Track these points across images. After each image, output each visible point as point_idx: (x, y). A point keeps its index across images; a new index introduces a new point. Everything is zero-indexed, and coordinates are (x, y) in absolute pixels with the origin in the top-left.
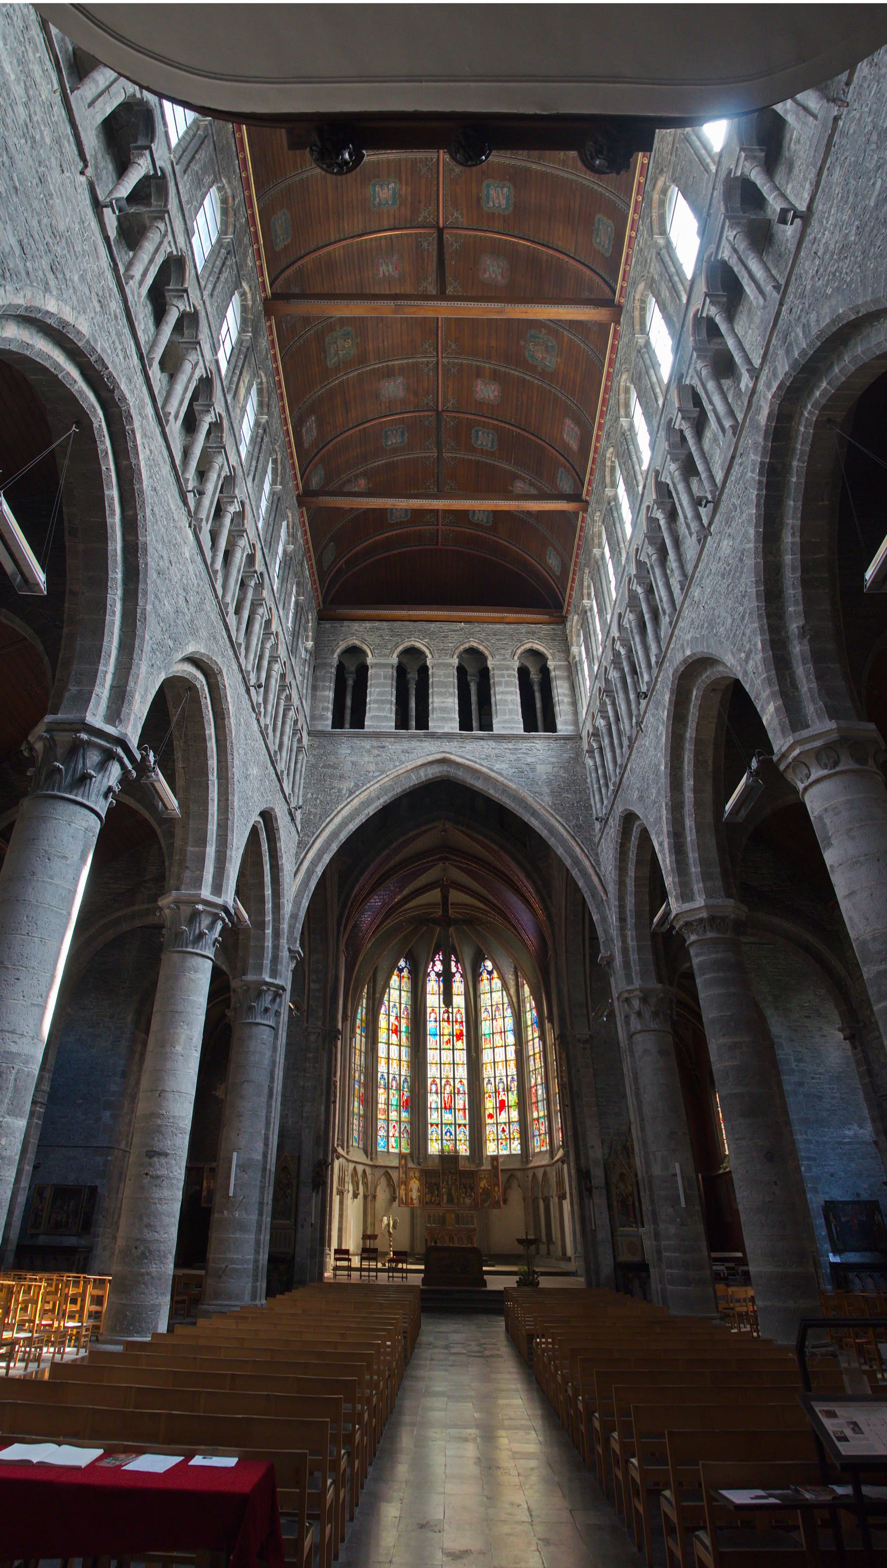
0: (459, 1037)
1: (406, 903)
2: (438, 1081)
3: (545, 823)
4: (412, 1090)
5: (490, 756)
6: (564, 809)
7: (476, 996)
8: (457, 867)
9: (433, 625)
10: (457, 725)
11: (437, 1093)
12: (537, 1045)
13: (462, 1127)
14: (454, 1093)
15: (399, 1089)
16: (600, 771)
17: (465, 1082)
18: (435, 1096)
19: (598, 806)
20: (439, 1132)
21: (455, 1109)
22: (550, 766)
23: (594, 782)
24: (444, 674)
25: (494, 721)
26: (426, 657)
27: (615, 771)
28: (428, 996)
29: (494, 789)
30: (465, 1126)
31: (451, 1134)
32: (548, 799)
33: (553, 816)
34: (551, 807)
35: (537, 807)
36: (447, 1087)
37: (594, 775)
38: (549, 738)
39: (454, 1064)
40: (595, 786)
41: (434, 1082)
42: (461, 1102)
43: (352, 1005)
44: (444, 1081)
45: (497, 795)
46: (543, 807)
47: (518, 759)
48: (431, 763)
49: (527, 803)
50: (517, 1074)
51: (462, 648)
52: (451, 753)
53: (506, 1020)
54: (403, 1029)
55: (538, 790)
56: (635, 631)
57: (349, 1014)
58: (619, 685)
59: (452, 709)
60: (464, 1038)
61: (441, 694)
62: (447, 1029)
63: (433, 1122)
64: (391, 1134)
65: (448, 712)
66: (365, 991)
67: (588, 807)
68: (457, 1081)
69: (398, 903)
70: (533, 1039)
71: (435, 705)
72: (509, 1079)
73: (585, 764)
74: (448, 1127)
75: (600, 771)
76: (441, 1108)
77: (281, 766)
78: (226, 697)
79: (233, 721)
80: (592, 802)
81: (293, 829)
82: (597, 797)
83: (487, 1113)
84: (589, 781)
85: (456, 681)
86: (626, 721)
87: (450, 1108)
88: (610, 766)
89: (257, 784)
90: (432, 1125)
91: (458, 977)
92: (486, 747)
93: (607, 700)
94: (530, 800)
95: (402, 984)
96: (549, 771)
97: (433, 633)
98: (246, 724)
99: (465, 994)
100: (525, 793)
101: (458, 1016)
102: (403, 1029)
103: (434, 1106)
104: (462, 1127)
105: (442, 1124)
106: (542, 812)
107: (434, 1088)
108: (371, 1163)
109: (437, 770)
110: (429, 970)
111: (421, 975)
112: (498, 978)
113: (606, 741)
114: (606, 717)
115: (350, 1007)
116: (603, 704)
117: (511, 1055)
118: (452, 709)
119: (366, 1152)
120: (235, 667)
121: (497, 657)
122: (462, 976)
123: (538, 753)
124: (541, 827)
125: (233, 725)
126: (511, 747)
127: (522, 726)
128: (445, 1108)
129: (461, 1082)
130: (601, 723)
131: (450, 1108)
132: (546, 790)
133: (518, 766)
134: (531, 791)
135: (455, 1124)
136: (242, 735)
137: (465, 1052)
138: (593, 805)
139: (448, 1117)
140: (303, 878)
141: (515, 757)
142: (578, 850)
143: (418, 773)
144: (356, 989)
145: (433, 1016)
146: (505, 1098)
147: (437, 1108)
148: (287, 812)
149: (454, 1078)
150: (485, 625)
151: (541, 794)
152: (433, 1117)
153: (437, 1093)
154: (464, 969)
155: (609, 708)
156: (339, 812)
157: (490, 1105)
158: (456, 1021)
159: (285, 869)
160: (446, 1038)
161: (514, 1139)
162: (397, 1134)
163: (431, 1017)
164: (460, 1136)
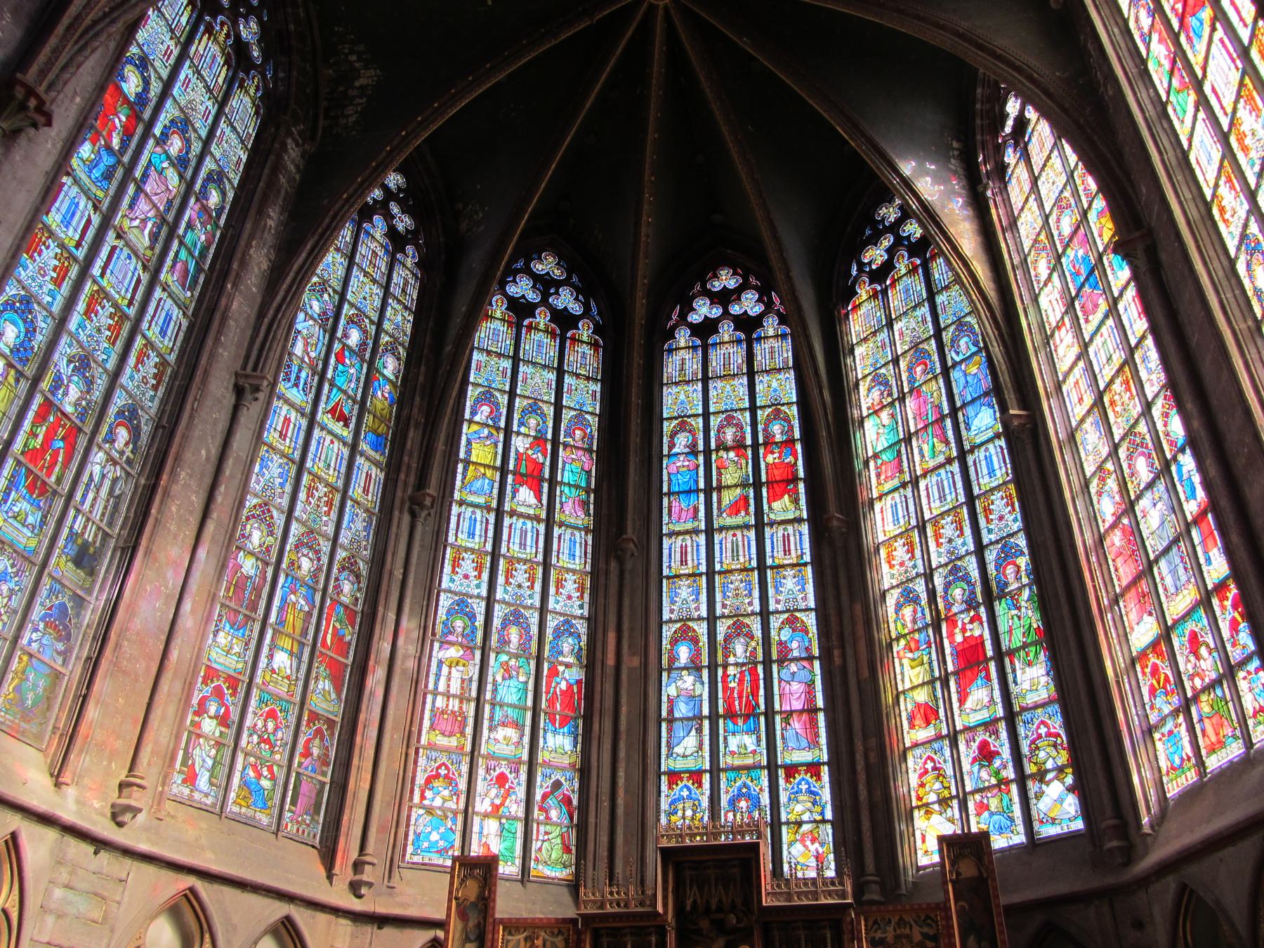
0: (782, 484)
2: (701, 629)
4: (591, 660)
7: (837, 350)
11: (695, 667)
13: (803, 778)
14: (767, 662)
17: (810, 620)
18: (688, 680)
21: (770, 714)
31: (757, 804)
36: (739, 648)
39: (762, 567)
41: (685, 634)
44: (722, 628)
50: (1028, 529)
53: (955, 375)
60: (801, 486)
62: (733, 471)
63: (679, 765)
64: (482, 805)
68: (775, 622)
74: (744, 778)
76: (714, 717)
87: (751, 713)
90: (674, 776)
101: (776, 429)
104: (803, 778)
105: (715, 771)
107: (684, 653)
108: (339, 895)
119: (328, 854)
128: (731, 715)
129: (792, 622)
135: (772, 767)
137: (805, 528)
149: (765, 614)
153: (695, 667)
154: (792, 299)
158: (769, 443)
160: (729, 497)
161: (1041, 776)
162: (517, 809)
164: (795, 808)
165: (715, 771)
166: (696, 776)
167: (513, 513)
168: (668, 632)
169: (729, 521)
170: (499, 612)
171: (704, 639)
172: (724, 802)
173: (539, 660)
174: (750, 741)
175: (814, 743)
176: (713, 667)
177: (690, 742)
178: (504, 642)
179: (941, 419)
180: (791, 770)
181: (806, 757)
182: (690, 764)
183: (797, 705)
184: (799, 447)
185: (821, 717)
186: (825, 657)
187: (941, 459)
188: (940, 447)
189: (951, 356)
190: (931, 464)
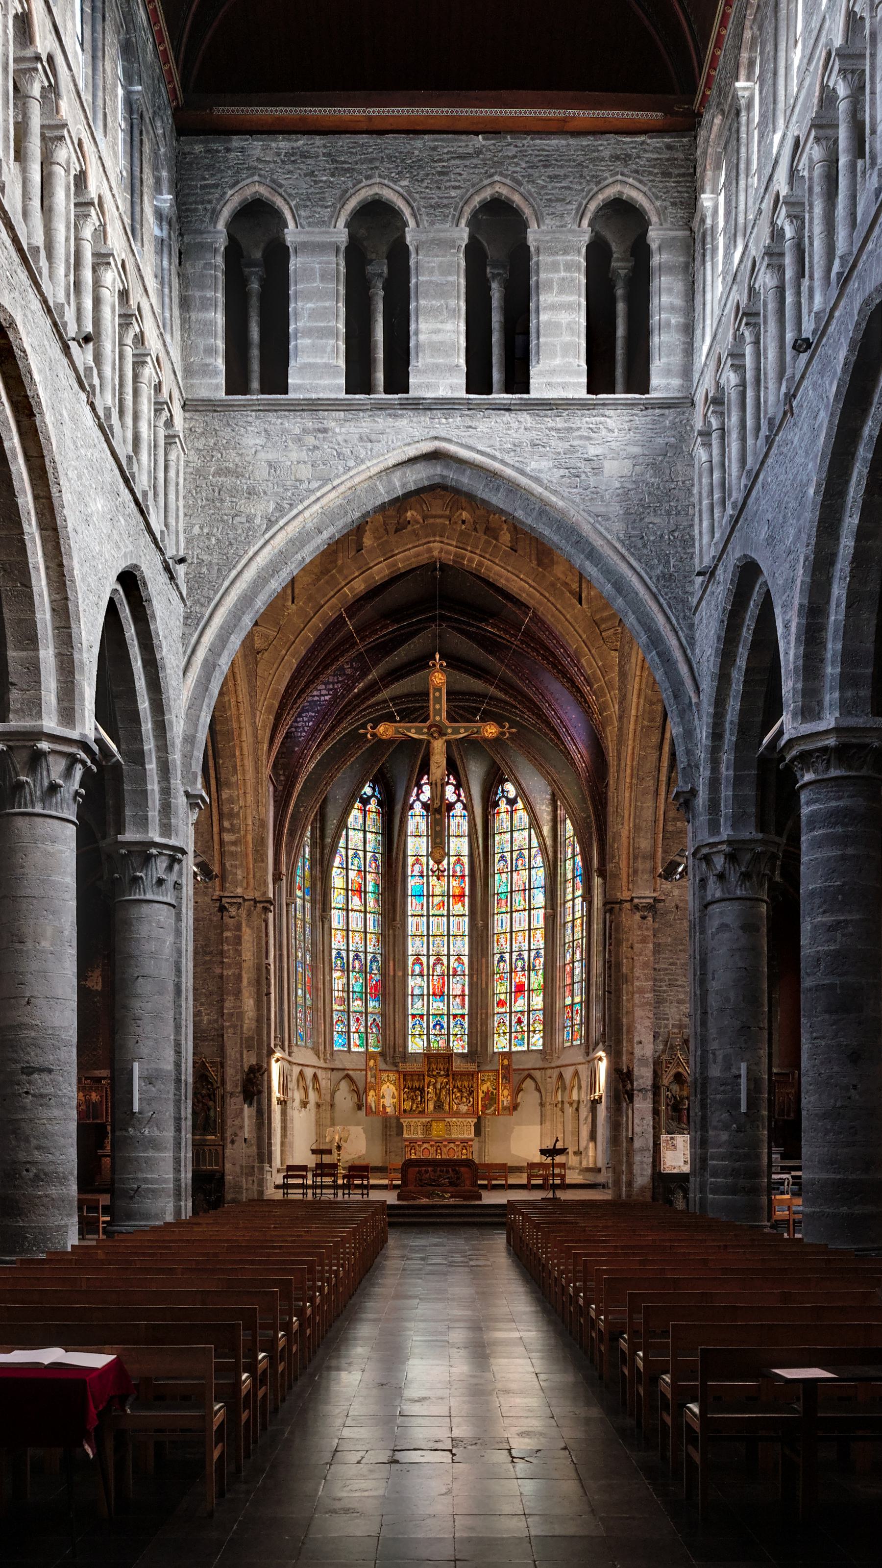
1: (373, 695)
3: (608, 572)
5: (519, 445)
6: (645, 546)
8: (462, 632)
9: (419, 143)
10: (461, 380)
12: (578, 907)
15: (364, 971)
16: (716, 475)
18: (419, 980)
19: (706, 539)
20: (425, 1025)
21: (448, 995)
22: (628, 463)
23: (705, 494)
24: (440, 266)
25: (533, 371)
26: (405, 224)
27: (740, 478)
28: (410, 840)
29: (524, 509)
30: (463, 1016)
32: (618, 527)
33: (623, 557)
34: (624, 545)
35: (598, 542)
37: (705, 481)
38: (632, 405)
40: (705, 502)
42: (459, 986)
43: (288, 854)
45: (529, 521)
46: (609, 542)
47: (573, 450)
48: (413, 461)
49: (580, 535)
51: (476, 201)
52: (449, 441)
54: (370, 888)
55: (602, 510)
56: (817, 189)
57: (284, 870)
58: (771, 306)
59: (454, 346)
61: (434, 312)
63: (415, 1012)
65: (447, 355)
66: (308, 834)
67: (688, 542)
69: (357, 696)
70: (573, 899)
71: (422, 337)
72: (533, 954)
73: (692, 458)
75: (716, 475)
76: (428, 995)
77: (142, 482)
78: (30, 372)
79: (49, 418)
80: (697, 532)
81: (174, 595)
82: (706, 524)
83: (496, 999)
84: (695, 491)
85: (463, 282)
86: (772, 385)
88: (734, 468)
89: (105, 527)
90: (414, 1016)
91: (459, 806)
92: (515, 425)
93: (747, 334)
94: (586, 529)
95: (368, 823)
96: (626, 472)
97: (419, 164)
98: (72, 419)
99: (469, 836)
100: (579, 517)
102: (370, 888)
103: (417, 991)
105: (428, 1015)
106: (607, 551)
109: (423, 475)
110: (412, 800)
111: (398, 808)
112: (525, 808)
113: (734, 420)
114: (739, 368)
115: (284, 859)
116: (739, 339)
117: (538, 920)
118: (454, 346)
120: (36, 304)
121: (548, 221)
122: (465, 808)
123: (610, 437)
124: (602, 579)
125: (50, 427)
126: (559, 426)
127: (584, 380)
128: (434, 995)
130: (731, 378)
131: (442, 995)
132: (616, 509)
133: (573, 462)
134: (589, 513)
135: (448, 1015)
136: (69, 443)
138: (697, 537)
139: (438, 1006)
140: (199, 677)
141: (567, 445)
142: (660, 619)
143: (390, 482)
144: (292, 834)
145: (417, 868)
146: (525, 980)
147: (422, 995)
148: (160, 567)
150: (528, 141)
151: (608, 519)
152: (416, 1007)
153: (421, 975)
155: (748, 350)
156: (251, 559)
157: (501, 989)
159: (168, 666)
163: (413, 870)
165: (428, 1015)
166: (421, 1016)
167: (352, 910)
168: (411, 959)
169: (437, 912)
170: (352, 955)
171: (425, 964)
172: (431, 1026)
173: (366, 973)
174: (441, 1005)
175: (463, 1007)
176: (428, 975)
177: (420, 1003)
178: (354, 968)
179: (524, 890)
180: (455, 1016)
181: (460, 1012)
182: (419, 1012)
183: (459, 993)
184: (467, 878)
185: (467, 998)
186: (471, 976)
187: (522, 908)
188: (522, 902)
189: (533, 862)
190: (519, 908)
